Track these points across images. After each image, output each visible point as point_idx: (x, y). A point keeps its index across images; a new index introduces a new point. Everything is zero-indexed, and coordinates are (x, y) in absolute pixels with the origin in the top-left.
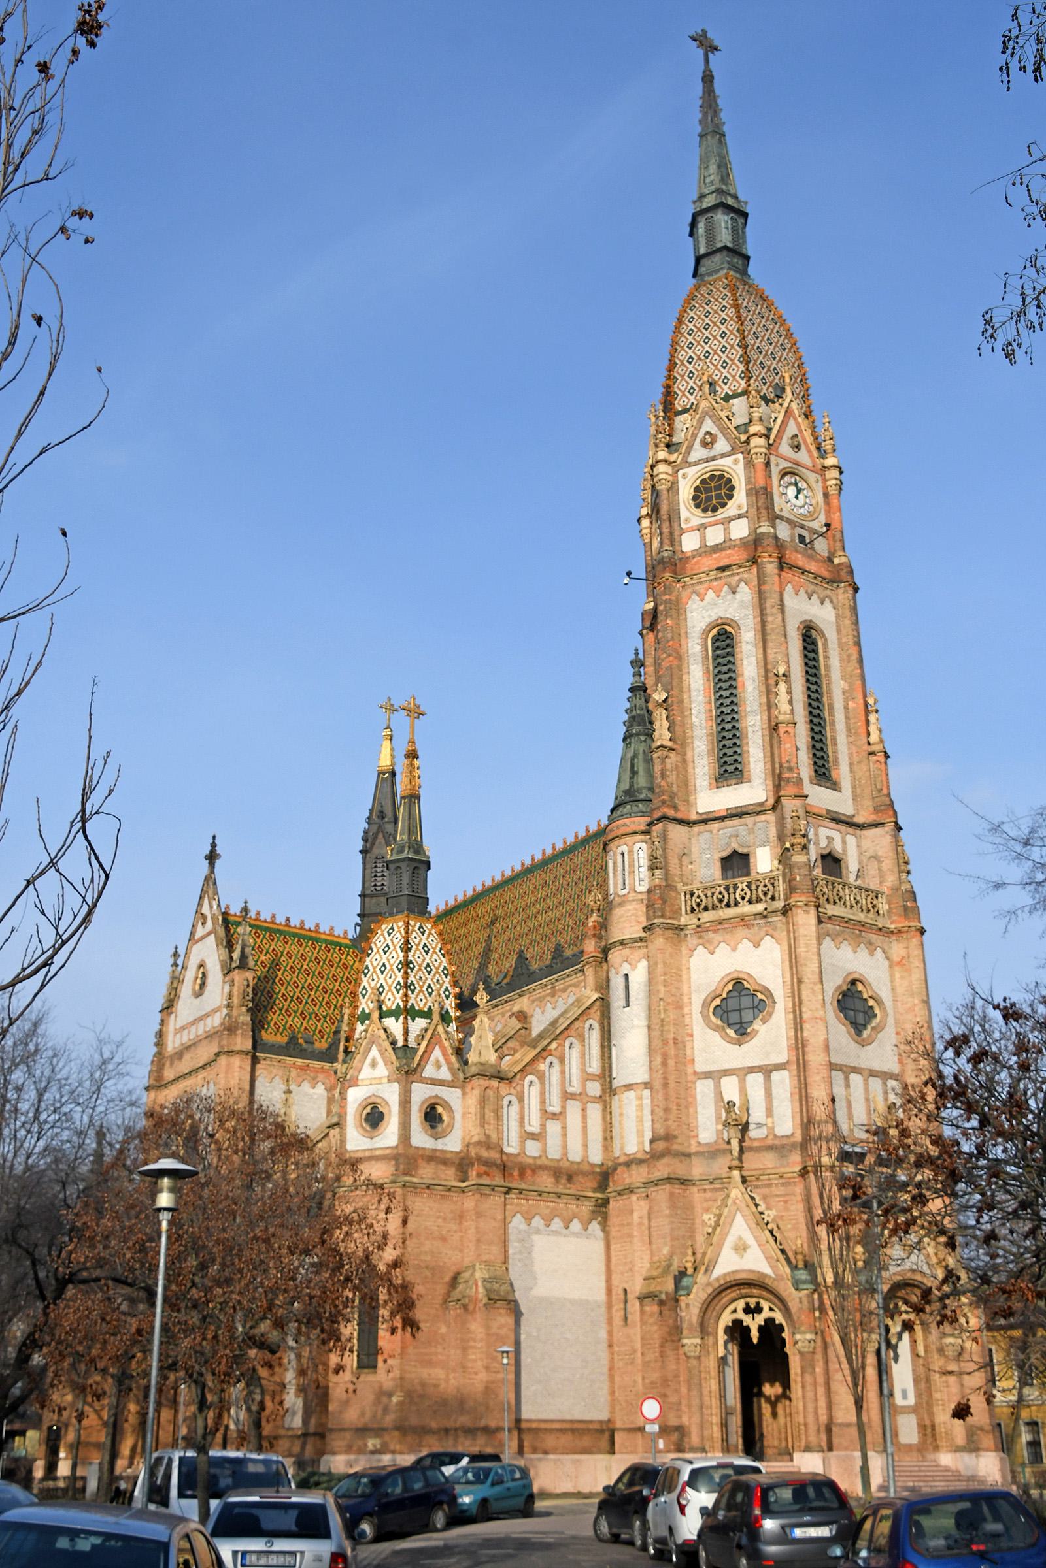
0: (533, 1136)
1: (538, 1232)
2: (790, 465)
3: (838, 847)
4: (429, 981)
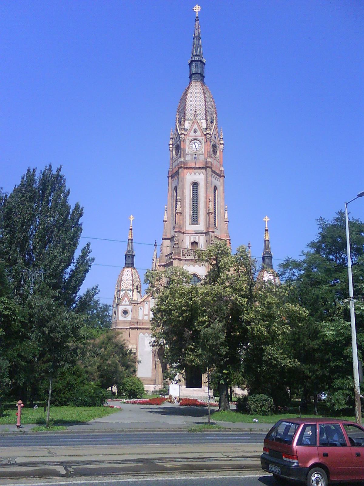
0: (146, 315)
1: (147, 337)
2: (194, 138)
3: (197, 240)
4: (127, 283)
